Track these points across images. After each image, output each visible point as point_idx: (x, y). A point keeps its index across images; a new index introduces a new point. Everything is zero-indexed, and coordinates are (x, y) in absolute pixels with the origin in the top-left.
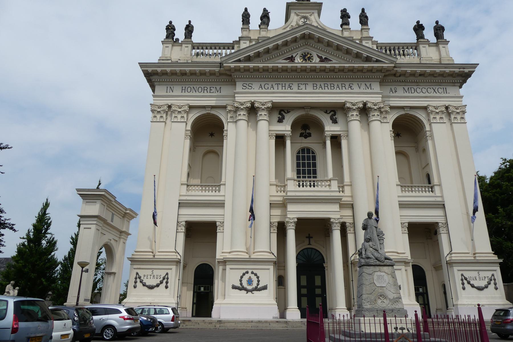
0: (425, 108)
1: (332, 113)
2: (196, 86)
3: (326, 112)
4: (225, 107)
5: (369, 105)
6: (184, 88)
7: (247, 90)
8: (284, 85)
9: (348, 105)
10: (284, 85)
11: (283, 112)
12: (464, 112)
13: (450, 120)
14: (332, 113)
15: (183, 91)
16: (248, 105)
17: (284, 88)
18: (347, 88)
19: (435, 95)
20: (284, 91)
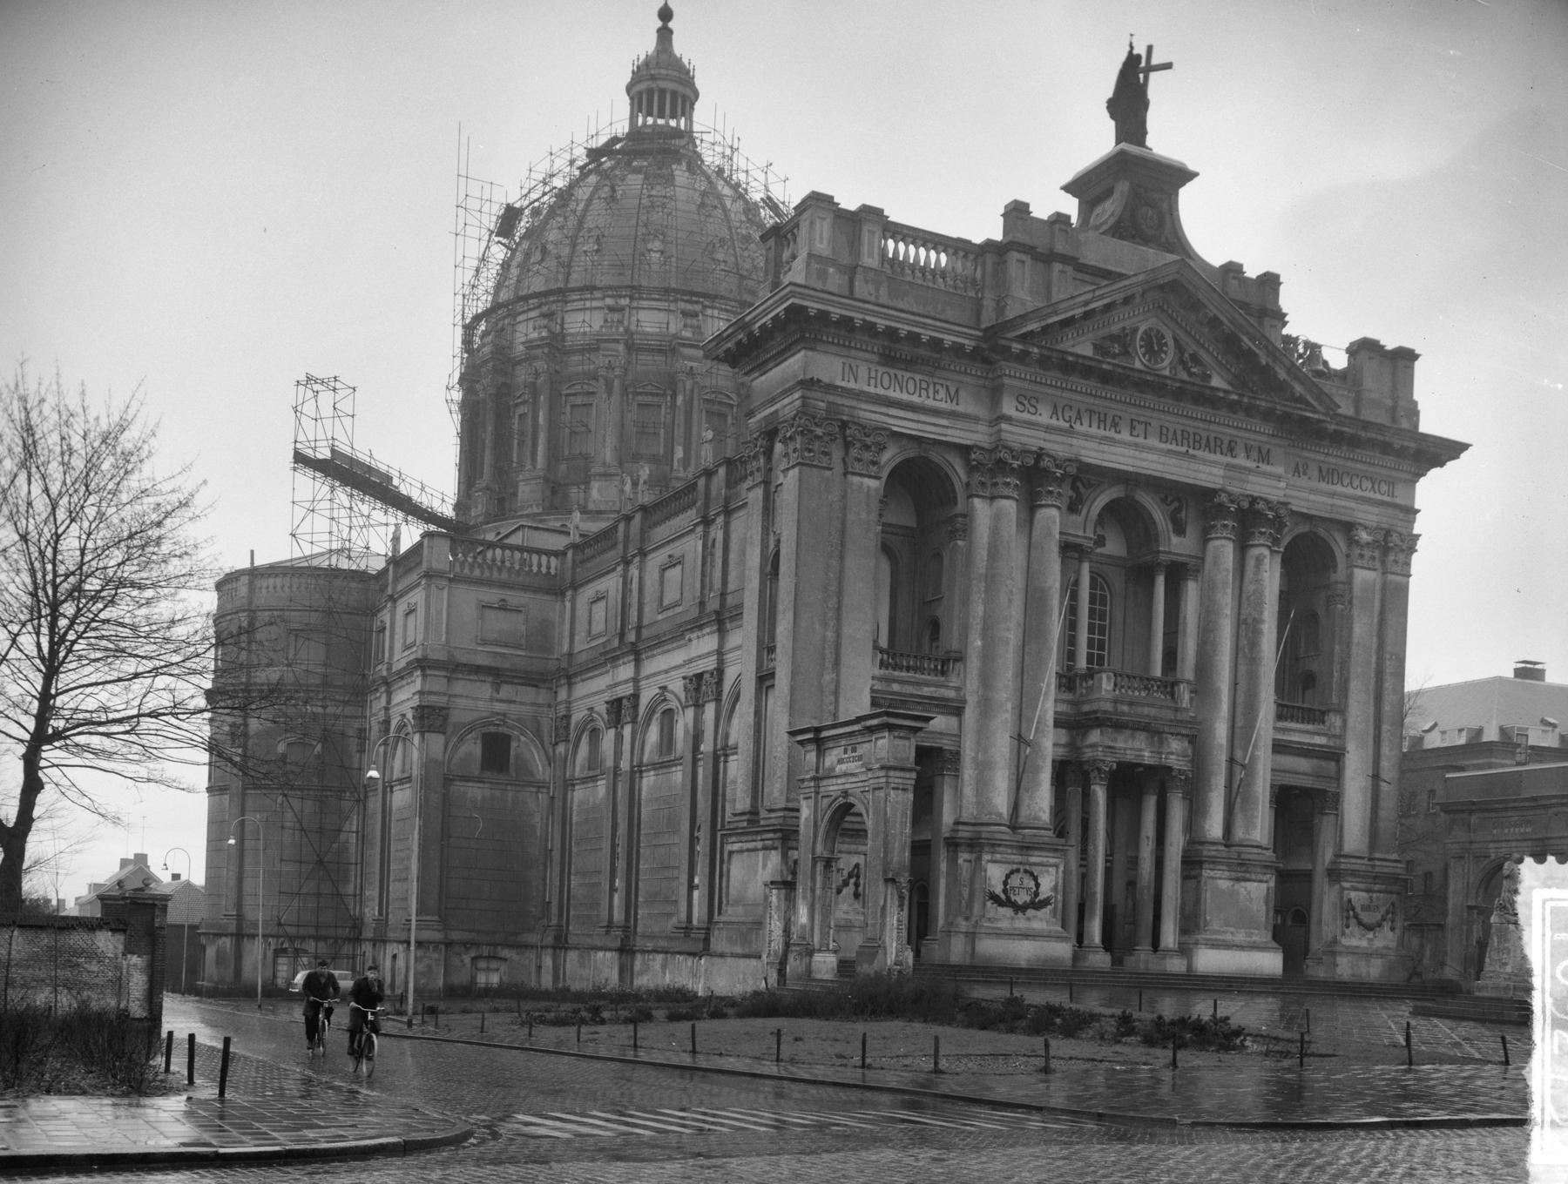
0: (1348, 527)
1: (1176, 504)
2: (904, 373)
3: (1164, 500)
4: (964, 450)
5: (1261, 506)
6: (873, 375)
7: (1025, 416)
8: (1102, 418)
9: (1224, 498)
10: (1102, 418)
11: (1079, 484)
12: (1412, 550)
13: (1383, 563)
14: (1176, 504)
15: (873, 381)
16: (1026, 460)
17: (1102, 426)
18: (1225, 451)
19: (1372, 495)
20: (1102, 432)
